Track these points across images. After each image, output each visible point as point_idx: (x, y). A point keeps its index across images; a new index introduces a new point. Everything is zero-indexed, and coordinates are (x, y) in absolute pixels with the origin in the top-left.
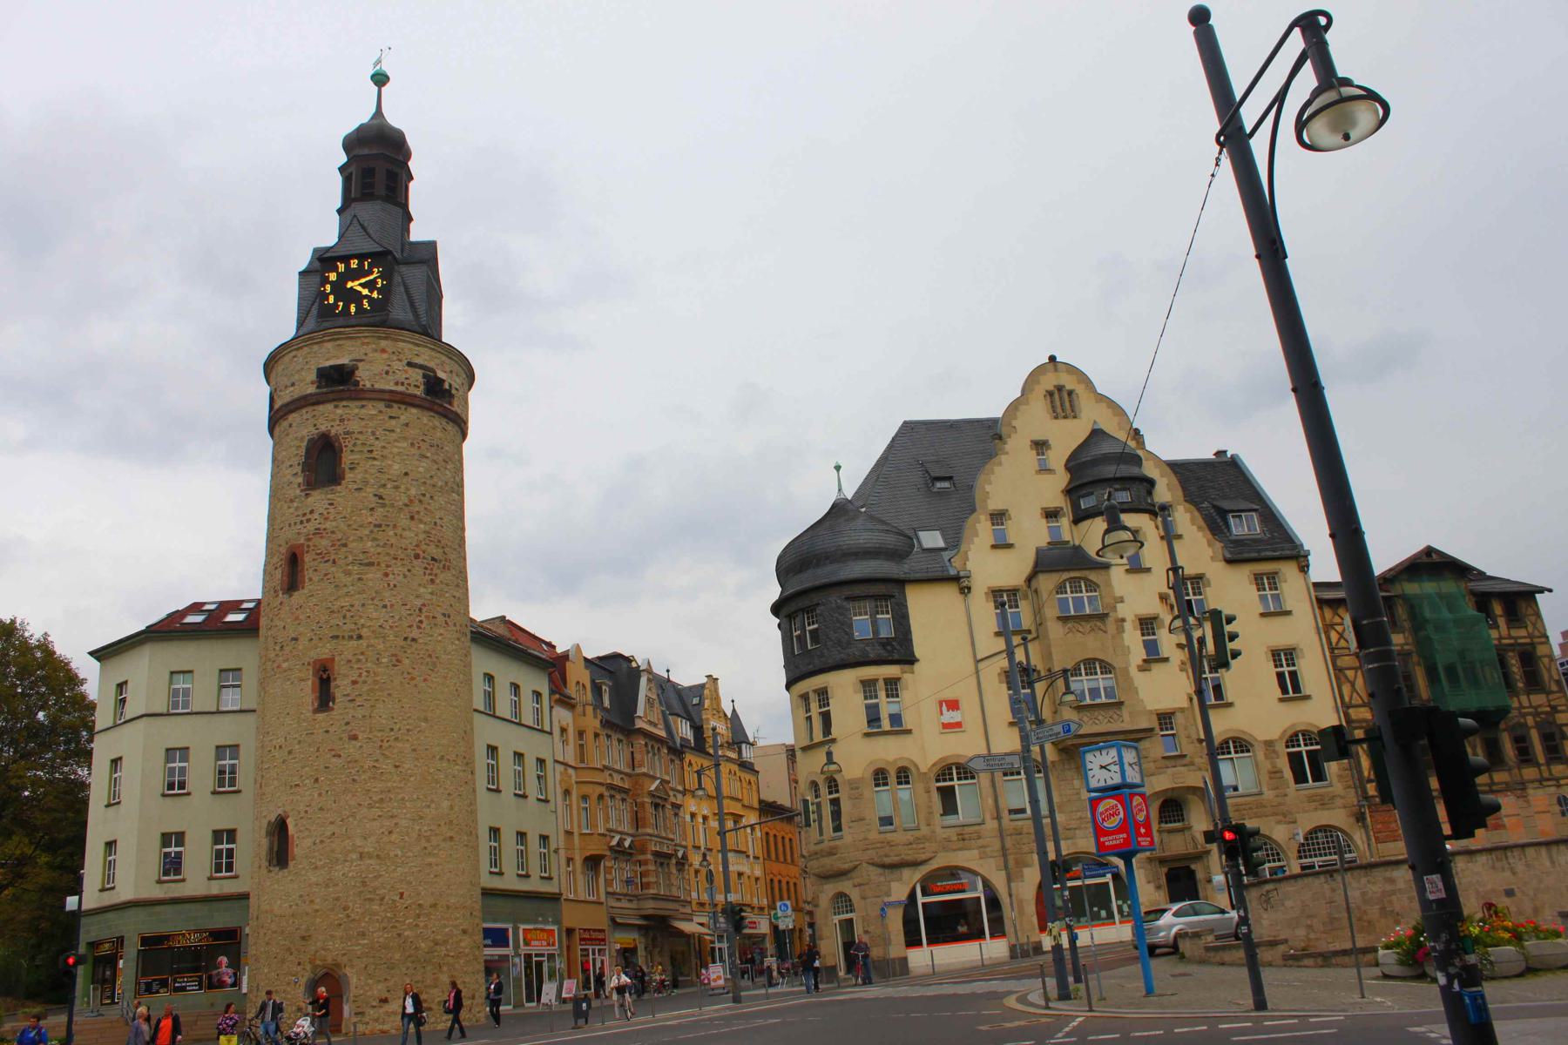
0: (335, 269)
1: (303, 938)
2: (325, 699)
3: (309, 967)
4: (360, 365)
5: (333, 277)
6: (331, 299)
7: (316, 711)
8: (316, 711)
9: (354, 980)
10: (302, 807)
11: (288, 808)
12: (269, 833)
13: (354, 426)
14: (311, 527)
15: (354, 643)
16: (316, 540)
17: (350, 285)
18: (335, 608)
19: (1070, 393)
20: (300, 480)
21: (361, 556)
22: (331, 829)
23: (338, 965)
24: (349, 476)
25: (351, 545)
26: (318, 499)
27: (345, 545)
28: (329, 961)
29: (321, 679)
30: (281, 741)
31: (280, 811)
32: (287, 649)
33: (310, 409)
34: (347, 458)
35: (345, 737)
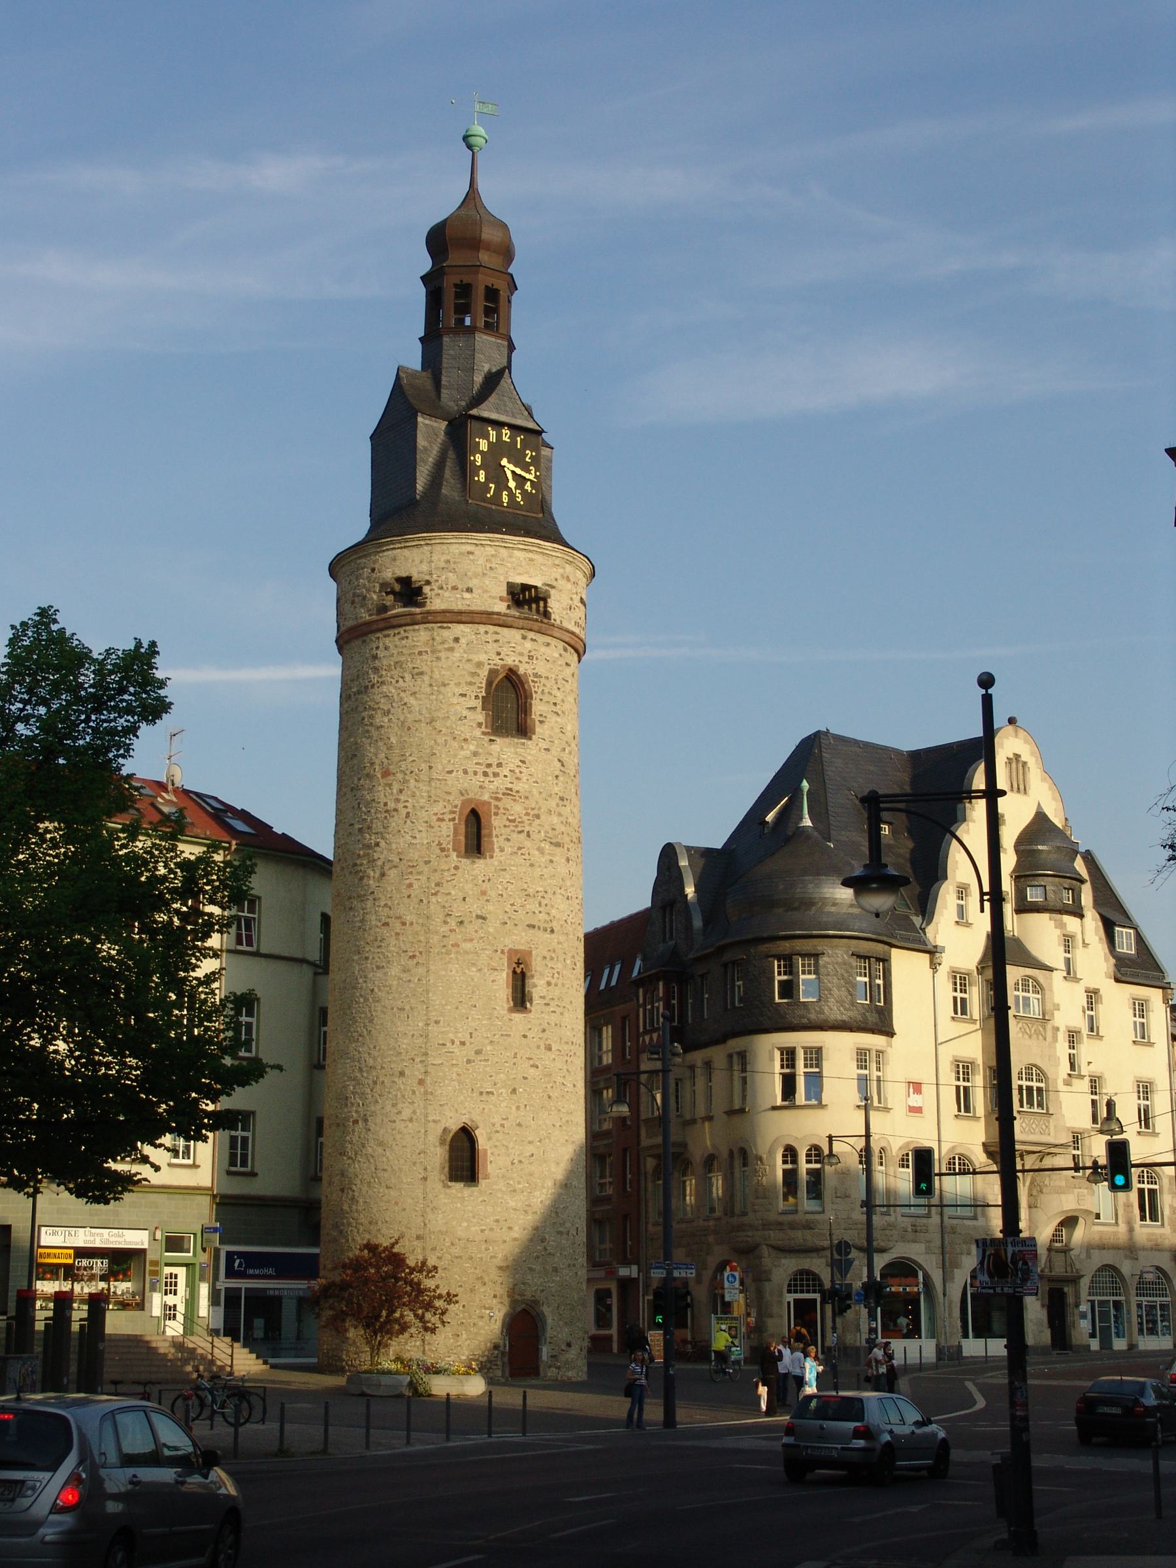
0: (487, 437)
2: (521, 998)
4: (552, 592)
5: (483, 445)
7: (511, 1010)
8: (511, 1010)
9: (550, 1321)
10: (497, 1120)
12: (442, 1142)
13: (541, 668)
14: (500, 784)
15: (548, 935)
16: (507, 802)
17: (504, 462)
18: (531, 891)
19: (1025, 764)
22: (530, 1149)
23: (536, 1302)
24: (538, 729)
25: (542, 817)
26: (506, 749)
27: (538, 816)
28: (528, 1295)
29: (514, 972)
30: (463, 1036)
32: (470, 928)
33: (491, 628)
34: (538, 708)
35: (542, 1047)
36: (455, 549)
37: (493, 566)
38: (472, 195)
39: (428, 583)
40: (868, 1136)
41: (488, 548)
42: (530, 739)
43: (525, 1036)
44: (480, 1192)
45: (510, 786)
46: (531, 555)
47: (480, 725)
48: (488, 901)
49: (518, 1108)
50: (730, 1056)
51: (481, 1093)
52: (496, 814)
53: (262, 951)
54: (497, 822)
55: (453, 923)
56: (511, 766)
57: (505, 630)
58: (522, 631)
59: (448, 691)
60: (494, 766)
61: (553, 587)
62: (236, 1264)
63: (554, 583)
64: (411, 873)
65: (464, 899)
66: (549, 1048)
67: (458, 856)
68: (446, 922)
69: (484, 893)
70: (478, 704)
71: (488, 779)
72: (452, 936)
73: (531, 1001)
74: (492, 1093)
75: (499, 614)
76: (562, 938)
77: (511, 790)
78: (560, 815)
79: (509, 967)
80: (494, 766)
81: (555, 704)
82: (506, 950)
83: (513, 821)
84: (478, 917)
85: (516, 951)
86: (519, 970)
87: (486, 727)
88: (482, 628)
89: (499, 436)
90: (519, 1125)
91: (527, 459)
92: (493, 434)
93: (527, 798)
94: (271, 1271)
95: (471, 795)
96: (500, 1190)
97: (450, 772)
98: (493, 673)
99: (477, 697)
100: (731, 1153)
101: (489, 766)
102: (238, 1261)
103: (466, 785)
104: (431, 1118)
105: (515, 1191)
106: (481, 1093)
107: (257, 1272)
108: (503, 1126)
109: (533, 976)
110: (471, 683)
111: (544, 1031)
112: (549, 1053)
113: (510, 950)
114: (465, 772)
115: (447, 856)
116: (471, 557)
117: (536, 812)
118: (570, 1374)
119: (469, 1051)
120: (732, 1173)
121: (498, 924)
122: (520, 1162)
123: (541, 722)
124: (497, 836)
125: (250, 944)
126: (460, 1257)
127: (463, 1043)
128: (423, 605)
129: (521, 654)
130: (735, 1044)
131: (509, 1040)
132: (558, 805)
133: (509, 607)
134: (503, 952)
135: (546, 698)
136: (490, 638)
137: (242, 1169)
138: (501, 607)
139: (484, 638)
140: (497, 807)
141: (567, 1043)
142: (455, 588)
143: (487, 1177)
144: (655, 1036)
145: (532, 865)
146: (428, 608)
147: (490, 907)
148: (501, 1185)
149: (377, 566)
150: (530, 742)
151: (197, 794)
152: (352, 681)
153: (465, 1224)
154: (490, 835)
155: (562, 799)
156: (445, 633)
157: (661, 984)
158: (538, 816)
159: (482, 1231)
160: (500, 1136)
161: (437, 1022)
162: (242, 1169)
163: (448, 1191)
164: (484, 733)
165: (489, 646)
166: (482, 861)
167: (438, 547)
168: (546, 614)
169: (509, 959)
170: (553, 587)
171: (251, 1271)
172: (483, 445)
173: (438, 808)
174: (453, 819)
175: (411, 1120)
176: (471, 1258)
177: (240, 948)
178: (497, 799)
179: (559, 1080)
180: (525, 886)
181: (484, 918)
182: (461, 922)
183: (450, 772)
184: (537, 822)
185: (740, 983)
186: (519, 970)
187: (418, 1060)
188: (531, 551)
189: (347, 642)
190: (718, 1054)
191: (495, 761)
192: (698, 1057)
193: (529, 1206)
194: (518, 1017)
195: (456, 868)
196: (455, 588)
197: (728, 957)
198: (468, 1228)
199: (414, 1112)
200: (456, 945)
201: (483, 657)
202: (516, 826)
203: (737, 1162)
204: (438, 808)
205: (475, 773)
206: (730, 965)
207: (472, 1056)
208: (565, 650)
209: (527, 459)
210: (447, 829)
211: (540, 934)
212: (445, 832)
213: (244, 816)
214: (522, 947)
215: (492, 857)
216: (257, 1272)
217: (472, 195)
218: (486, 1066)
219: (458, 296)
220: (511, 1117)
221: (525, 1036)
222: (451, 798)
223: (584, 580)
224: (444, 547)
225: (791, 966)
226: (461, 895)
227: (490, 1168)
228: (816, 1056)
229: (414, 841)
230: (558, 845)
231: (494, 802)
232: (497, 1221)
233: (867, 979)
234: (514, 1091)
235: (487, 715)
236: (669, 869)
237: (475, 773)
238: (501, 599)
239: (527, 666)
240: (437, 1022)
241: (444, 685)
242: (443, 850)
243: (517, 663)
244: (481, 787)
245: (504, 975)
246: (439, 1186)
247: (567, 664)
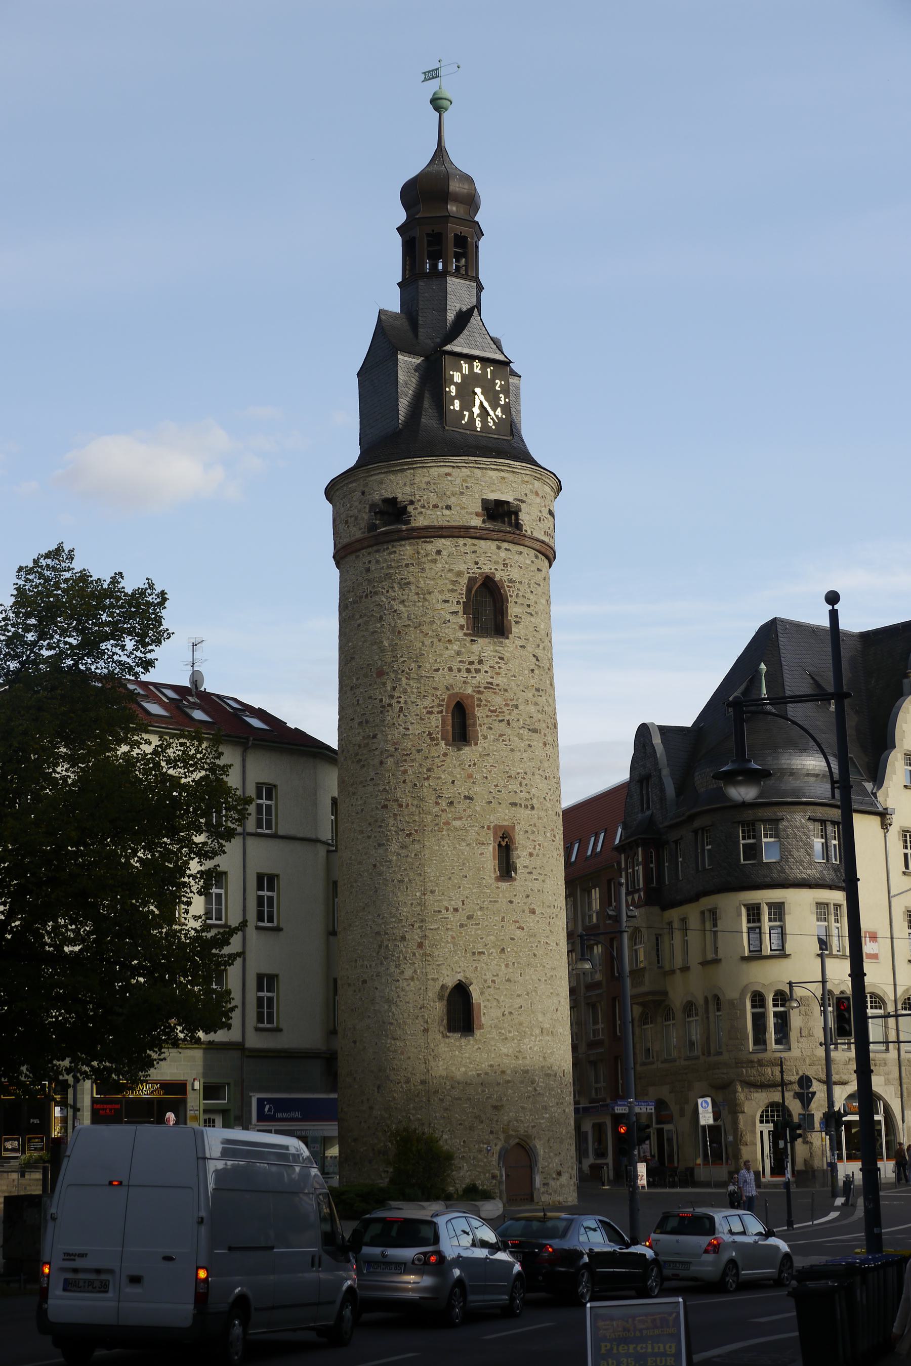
0: (460, 369)
1: (495, 1108)
3: (502, 1137)
4: (523, 506)
6: (457, 405)
9: (541, 1152)
10: (489, 977)
12: (441, 998)
13: (515, 574)
16: (488, 695)
17: (478, 390)
18: (512, 773)
20: (462, 621)
21: (528, 721)
22: (519, 1001)
23: (529, 1137)
24: (514, 629)
25: (521, 707)
28: (522, 1131)
29: (500, 845)
31: (460, 977)
32: (460, 807)
34: (513, 610)
35: (527, 911)
36: (435, 472)
37: (469, 485)
38: (440, 153)
39: (412, 502)
40: (824, 982)
41: (464, 470)
42: (508, 638)
43: (511, 902)
44: (476, 1040)
45: (490, 680)
46: (502, 474)
47: (462, 627)
48: (474, 783)
49: (507, 966)
50: (703, 913)
51: (474, 954)
52: (479, 706)
53: (280, 833)
54: (479, 713)
55: (444, 804)
56: (491, 663)
57: (482, 542)
58: (497, 542)
59: (433, 598)
60: (476, 663)
61: (523, 502)
62: (266, 1109)
63: (524, 498)
64: (405, 761)
65: (453, 782)
66: (533, 912)
67: (446, 745)
68: (437, 803)
69: (470, 776)
70: (460, 608)
71: (471, 675)
72: (444, 815)
73: (515, 871)
74: (483, 953)
75: (475, 528)
76: (542, 814)
77: (491, 684)
78: (536, 704)
79: (495, 842)
80: (476, 663)
81: (529, 606)
82: (492, 825)
83: (495, 711)
84: (466, 797)
85: (501, 827)
86: (504, 844)
87: (468, 629)
88: (461, 541)
89: (471, 368)
90: (508, 980)
91: (497, 388)
92: (465, 367)
93: (506, 690)
94: (297, 1115)
95: (457, 690)
96: (493, 1038)
97: (437, 670)
98: (472, 580)
99: (458, 603)
100: (706, 1000)
101: (472, 663)
102: (267, 1107)
103: (451, 681)
104: (430, 977)
105: (506, 1039)
106: (474, 954)
107: (285, 1115)
109: (517, 849)
110: (453, 591)
111: (528, 896)
112: (533, 916)
113: (495, 827)
114: (450, 669)
115: (436, 745)
116: (449, 478)
117: (514, 702)
118: (560, 1199)
119: (461, 916)
120: (708, 1018)
121: (484, 803)
122: (511, 1013)
123: (517, 622)
124: (480, 725)
125: (269, 827)
126: (460, 1099)
127: (456, 910)
128: (408, 522)
129: (496, 563)
130: (707, 902)
131: (497, 905)
132: (534, 696)
133: (484, 522)
134: (489, 828)
135: (520, 601)
136: (468, 549)
137: (269, 1026)
138: (477, 522)
139: (463, 549)
140: (479, 700)
141: (549, 907)
142: (436, 506)
143: (481, 1027)
144: (636, 896)
145: (512, 750)
147: (477, 789)
148: (494, 1034)
149: (366, 490)
150: (507, 641)
151: (218, 696)
152: (349, 592)
154: (474, 725)
155: (538, 690)
156: (429, 547)
157: (640, 849)
158: (516, 707)
160: (492, 991)
161: (432, 892)
162: (269, 1026)
163: (447, 1040)
164: (465, 635)
165: (468, 557)
166: (467, 748)
168: (518, 526)
169: (495, 834)
170: (523, 502)
171: (279, 1115)
172: (457, 377)
173: (427, 702)
174: (441, 712)
175: (412, 979)
176: (469, 1099)
177: (260, 831)
178: (480, 692)
179: (543, 940)
180: (507, 768)
181: (471, 799)
182: (452, 803)
183: (437, 670)
184: (516, 711)
185: (710, 847)
186: (504, 844)
187: (417, 925)
188: (502, 471)
189: (343, 558)
190: (692, 912)
191: (474, 658)
192: (674, 914)
193: (520, 1052)
194: (504, 885)
195: (445, 755)
196: (436, 506)
197: (697, 824)
199: (415, 971)
201: (463, 567)
202: (497, 716)
203: (712, 1007)
204: (427, 702)
205: (459, 670)
206: (700, 832)
208: (537, 557)
209: (497, 388)
210: (435, 721)
211: (522, 810)
212: (434, 723)
213: (261, 714)
214: (506, 823)
215: (476, 744)
216: (285, 1115)
217: (440, 153)
218: (477, 930)
219: (430, 244)
220: (501, 974)
221: (511, 902)
222: (439, 693)
223: (552, 494)
224: (425, 470)
225: (754, 830)
226: (450, 779)
228: (778, 911)
229: (407, 732)
230: (535, 731)
231: (476, 696)
233: (823, 840)
234: (503, 950)
235: (468, 618)
236: (644, 746)
237: (459, 670)
238: (477, 514)
239: (502, 573)
240: (432, 892)
241: (430, 593)
242: (432, 739)
243: (493, 570)
244: (465, 682)
245: (491, 848)
246: (439, 1037)
247: (538, 570)
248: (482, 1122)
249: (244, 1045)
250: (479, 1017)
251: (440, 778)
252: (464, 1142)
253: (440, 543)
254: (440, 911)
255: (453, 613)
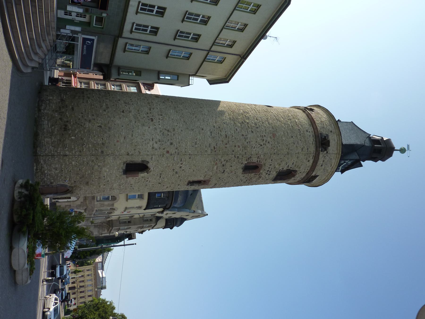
11: (151, 173)
12: (143, 161)
30: (183, 167)
31: (152, 169)
36: (333, 161)
39: (327, 152)
44: (121, 175)
51: (161, 174)
55: (224, 163)
62: (88, 42)
64: (243, 147)
65: (231, 166)
70: (289, 168)
83: (251, 179)
84: (224, 171)
88: (309, 168)
90: (146, 185)
94: (85, 53)
95: (263, 167)
102: (90, 42)
106: (161, 174)
107: (85, 48)
108: (147, 181)
126: (93, 169)
127: (181, 167)
128: (322, 151)
146: (321, 153)
149: (332, 133)
153: (107, 170)
154: (249, 173)
156: (311, 157)
159: (104, 177)
161: (190, 158)
167: (336, 156)
171: (85, 46)
173: (262, 156)
174: (257, 162)
175: (153, 148)
176: (93, 173)
181: (223, 173)
182: (224, 166)
183: (272, 161)
187: (176, 151)
196: (324, 161)
198: (106, 171)
199: (156, 149)
200: (216, 164)
205: (269, 168)
207: (175, 171)
212: (254, 159)
216: (85, 48)
227: (130, 178)
232: (108, 181)
234: (160, 183)
240: (190, 158)
242: (249, 158)
246: (125, 160)
248: (80, 178)
249: (121, 37)
250: (132, 176)
251: (234, 161)
252: (70, 171)
253: (311, 161)
254: (181, 161)
255: (288, 166)
